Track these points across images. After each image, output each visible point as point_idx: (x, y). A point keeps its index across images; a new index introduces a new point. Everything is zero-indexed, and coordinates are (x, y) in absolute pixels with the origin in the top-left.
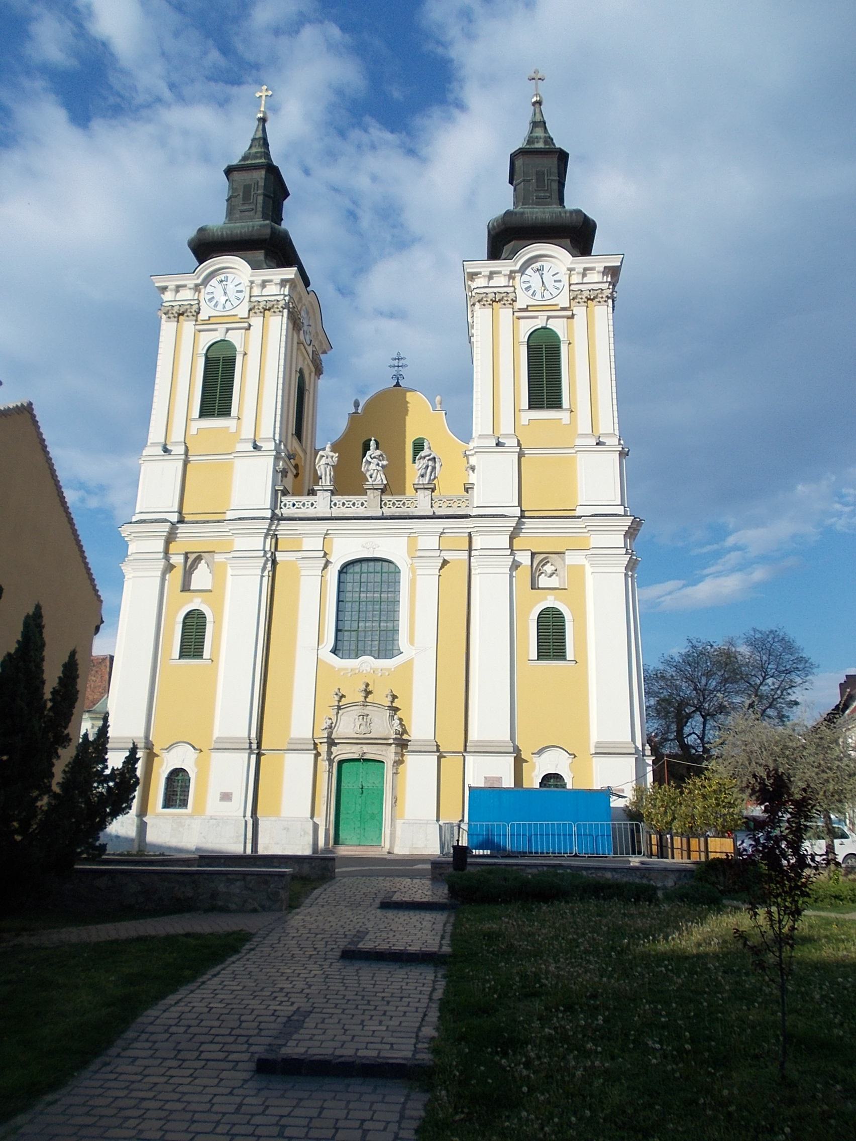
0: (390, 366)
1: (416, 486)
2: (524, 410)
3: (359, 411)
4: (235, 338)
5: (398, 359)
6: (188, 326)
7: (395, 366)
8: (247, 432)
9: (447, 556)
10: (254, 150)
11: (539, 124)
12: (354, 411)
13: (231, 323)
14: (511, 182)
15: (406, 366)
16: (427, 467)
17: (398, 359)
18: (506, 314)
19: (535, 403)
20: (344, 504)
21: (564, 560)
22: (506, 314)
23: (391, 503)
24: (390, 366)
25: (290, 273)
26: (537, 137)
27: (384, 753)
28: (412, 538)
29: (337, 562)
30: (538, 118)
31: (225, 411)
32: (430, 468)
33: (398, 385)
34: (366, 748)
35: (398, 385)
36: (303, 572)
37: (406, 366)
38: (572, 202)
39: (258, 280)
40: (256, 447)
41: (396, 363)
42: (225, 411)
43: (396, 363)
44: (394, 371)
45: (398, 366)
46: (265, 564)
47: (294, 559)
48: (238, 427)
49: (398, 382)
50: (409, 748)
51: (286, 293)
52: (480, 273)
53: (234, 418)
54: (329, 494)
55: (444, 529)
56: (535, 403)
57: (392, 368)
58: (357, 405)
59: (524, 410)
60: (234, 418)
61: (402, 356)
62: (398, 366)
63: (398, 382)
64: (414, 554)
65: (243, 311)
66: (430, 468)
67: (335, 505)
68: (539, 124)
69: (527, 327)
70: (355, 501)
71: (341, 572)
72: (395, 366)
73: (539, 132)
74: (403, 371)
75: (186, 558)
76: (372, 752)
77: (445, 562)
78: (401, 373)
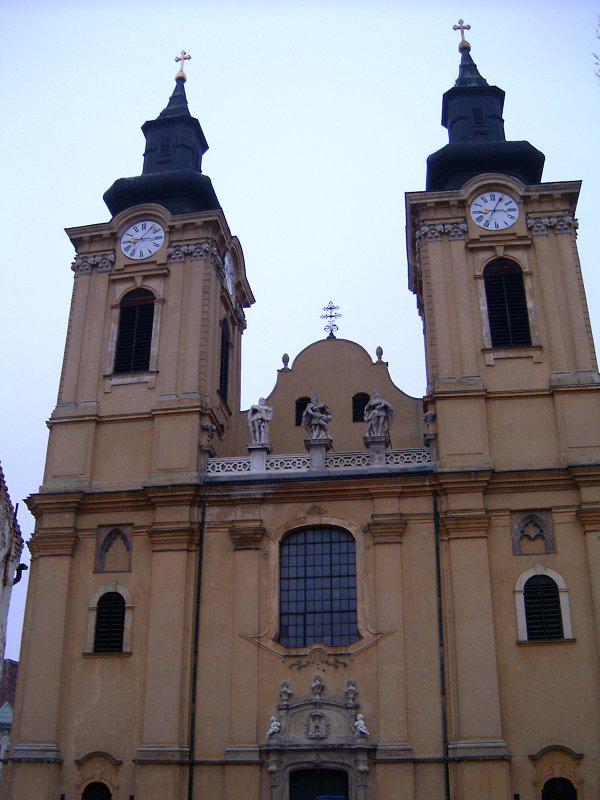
0: (323, 317)
3: (290, 366)
4: (155, 285)
5: (331, 308)
10: (172, 107)
11: (468, 66)
12: (283, 366)
14: (444, 123)
15: (340, 315)
16: (379, 417)
17: (331, 308)
22: (458, 247)
24: (323, 317)
25: (212, 217)
26: (469, 79)
27: (346, 761)
30: (468, 63)
32: (382, 420)
33: (332, 337)
34: (324, 757)
35: (332, 337)
37: (340, 315)
38: (513, 132)
39: (179, 224)
41: (328, 313)
43: (328, 313)
44: (326, 322)
45: (331, 316)
49: (331, 334)
50: (379, 756)
55: (404, 487)
58: (286, 359)
60: (152, 373)
62: (331, 316)
63: (331, 334)
66: (382, 420)
68: (468, 66)
70: (295, 460)
71: (282, 544)
73: (468, 75)
74: (337, 321)
76: (330, 761)
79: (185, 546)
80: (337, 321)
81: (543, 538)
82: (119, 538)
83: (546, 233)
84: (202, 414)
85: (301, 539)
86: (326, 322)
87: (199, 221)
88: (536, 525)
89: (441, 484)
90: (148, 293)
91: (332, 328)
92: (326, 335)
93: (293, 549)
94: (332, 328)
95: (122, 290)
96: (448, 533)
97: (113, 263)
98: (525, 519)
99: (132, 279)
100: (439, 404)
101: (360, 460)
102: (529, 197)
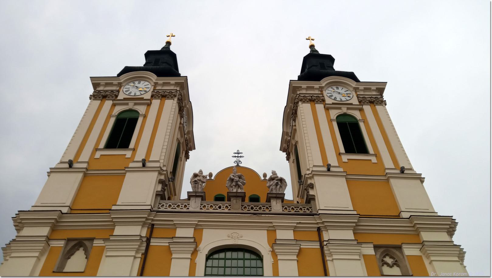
1: (270, 195)
2: (343, 154)
3: (213, 178)
4: (141, 109)
5: (238, 153)
6: (108, 103)
7: (235, 157)
8: (140, 155)
9: (304, 245)
13: (138, 100)
15: (243, 157)
17: (238, 153)
18: (320, 107)
19: (349, 150)
20: (211, 206)
21: (402, 253)
23: (250, 207)
28: (272, 231)
29: (205, 248)
31: (125, 145)
33: (238, 165)
35: (238, 165)
36: (174, 256)
39: (160, 82)
40: (144, 165)
41: (237, 155)
42: (125, 145)
43: (237, 155)
45: (238, 157)
46: (140, 246)
47: (168, 244)
48: (133, 155)
51: (178, 89)
52: (301, 87)
53: (131, 149)
54: (200, 199)
56: (349, 150)
57: (234, 158)
59: (343, 154)
60: (131, 149)
61: (240, 152)
62: (238, 157)
64: (274, 243)
65: (148, 96)
67: (205, 206)
69: (334, 114)
70: (221, 205)
71: (208, 258)
72: (235, 157)
74: (241, 159)
75: (67, 245)
77: (300, 250)
78: (239, 160)
79: (133, 253)
80: (241, 159)
81: (398, 266)
82: (81, 249)
83: (369, 104)
84: (160, 174)
85: (222, 255)
86: (235, 159)
87: (173, 82)
88: (391, 257)
89: (323, 223)
90: (137, 112)
91: (238, 162)
92: (236, 165)
93: (215, 263)
94: (238, 162)
95: (118, 109)
96: (332, 256)
97: (117, 96)
98: (382, 253)
99: (127, 104)
100: (316, 178)
101: (265, 208)
102: (358, 88)
